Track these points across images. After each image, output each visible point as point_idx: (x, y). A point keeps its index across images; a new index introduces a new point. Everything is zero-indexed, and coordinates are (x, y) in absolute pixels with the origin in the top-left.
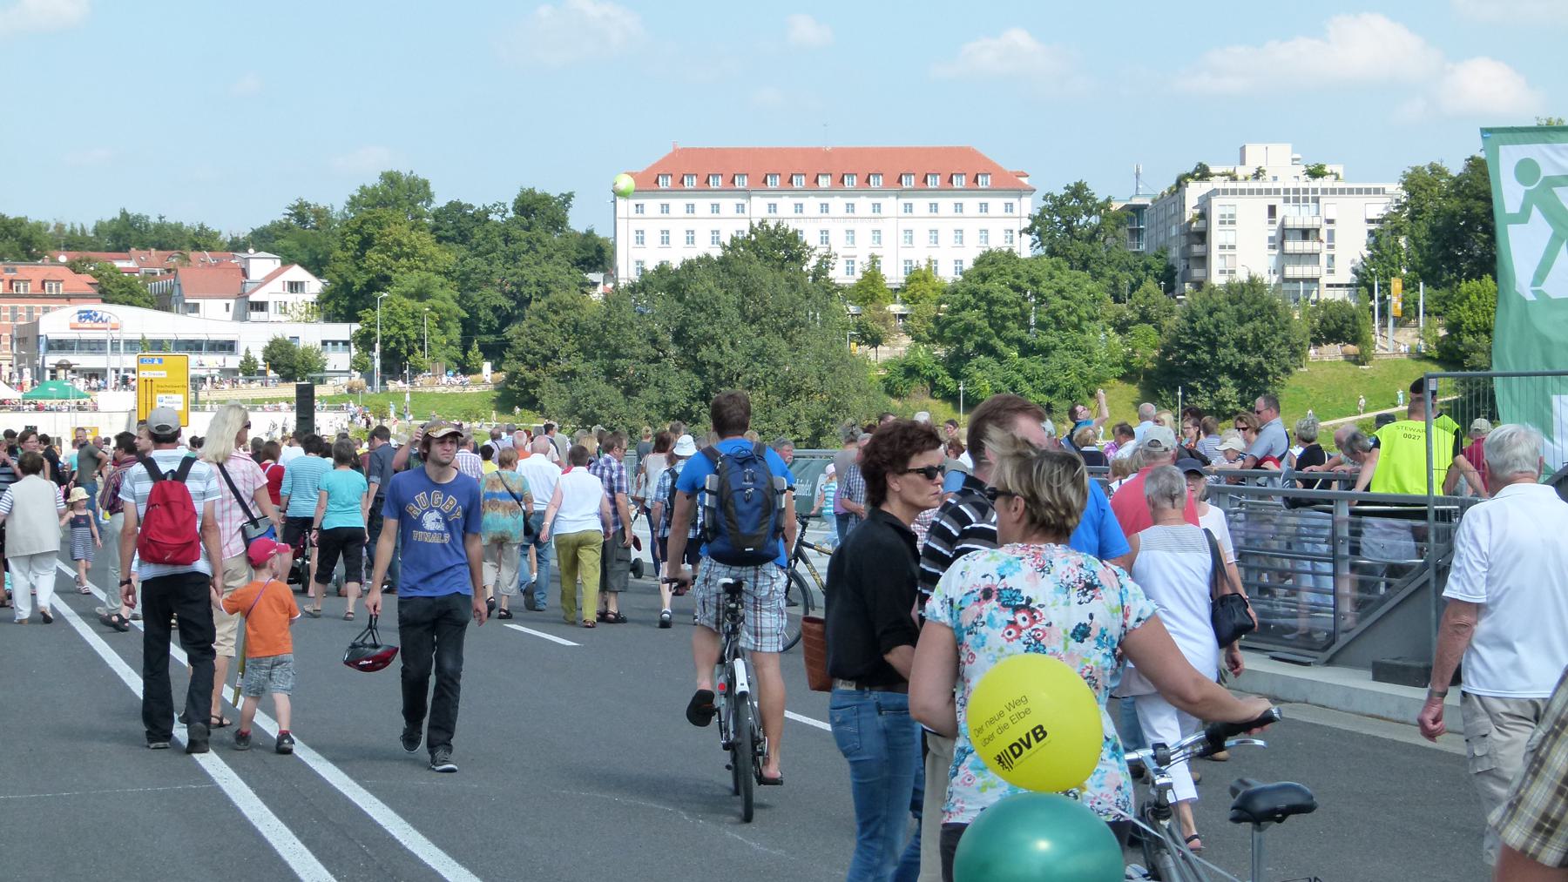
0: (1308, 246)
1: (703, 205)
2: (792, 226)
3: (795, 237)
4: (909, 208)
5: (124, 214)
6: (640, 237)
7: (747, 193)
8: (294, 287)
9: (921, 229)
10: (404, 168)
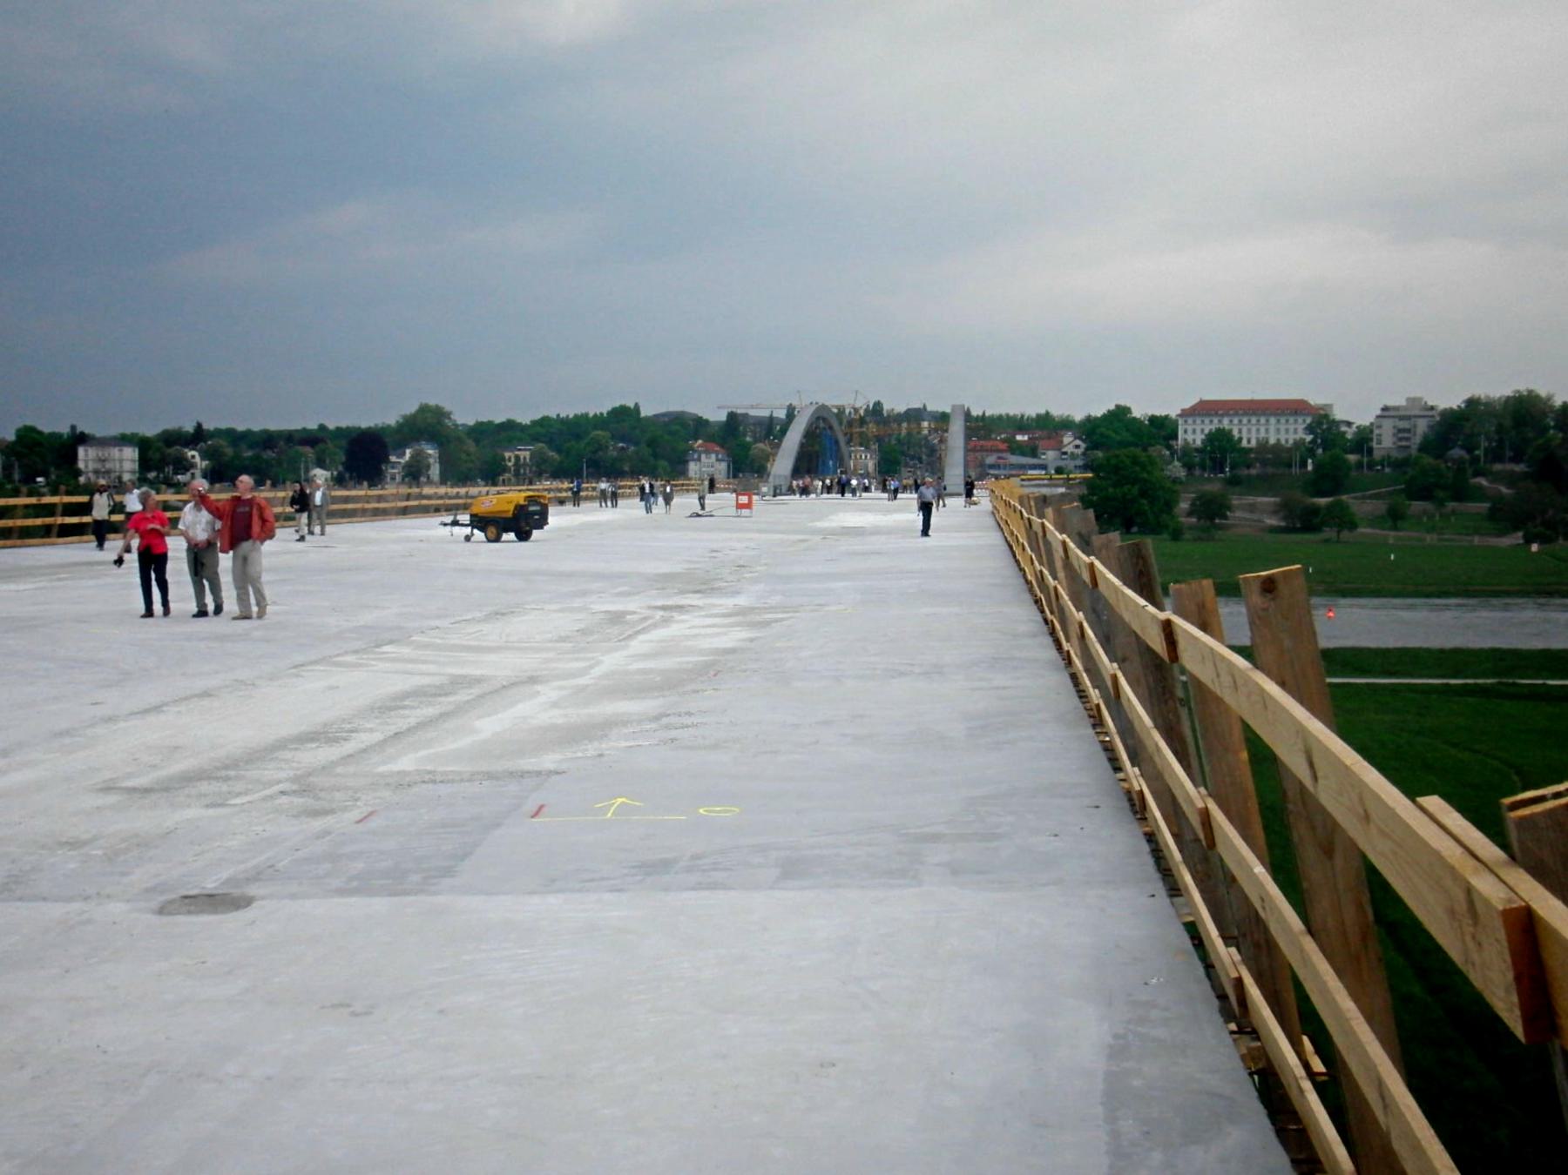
0: (1406, 435)
1: (1207, 421)
2: (1227, 427)
3: (1230, 431)
4: (1278, 421)
5: (1047, 413)
6: (1186, 431)
7: (1222, 415)
8: (1077, 447)
9: (1283, 428)
10: (1122, 403)
